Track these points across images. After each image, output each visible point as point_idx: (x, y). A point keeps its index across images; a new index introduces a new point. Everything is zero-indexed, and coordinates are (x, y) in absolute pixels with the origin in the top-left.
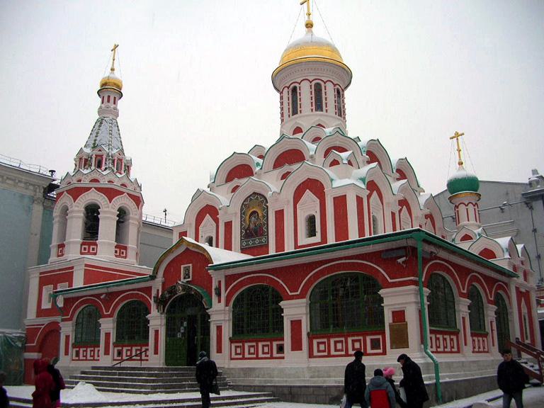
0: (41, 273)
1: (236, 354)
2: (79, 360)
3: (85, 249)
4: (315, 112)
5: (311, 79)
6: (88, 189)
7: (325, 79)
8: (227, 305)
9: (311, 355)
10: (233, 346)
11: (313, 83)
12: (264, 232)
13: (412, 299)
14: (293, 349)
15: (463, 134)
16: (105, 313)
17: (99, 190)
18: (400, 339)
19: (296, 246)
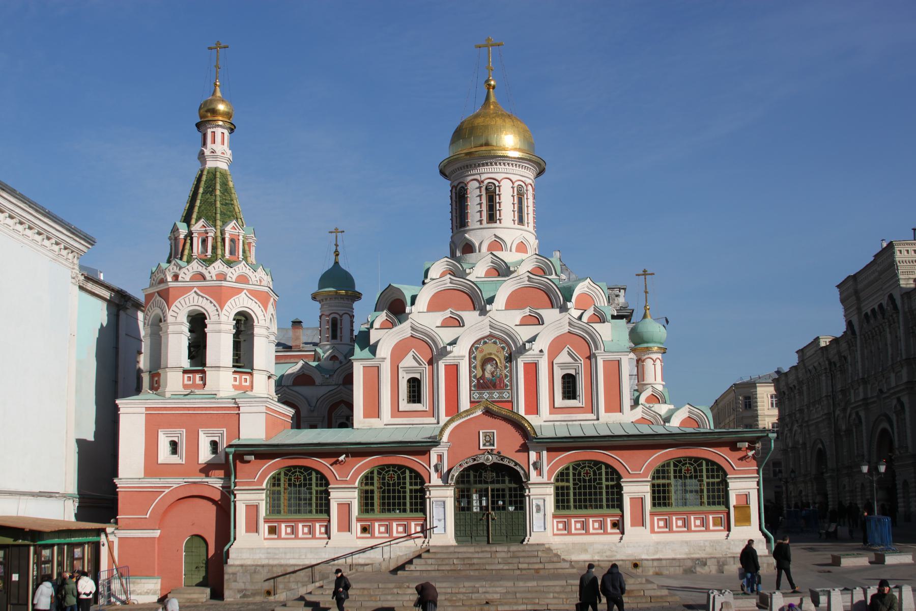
0: (146, 408)
1: (558, 529)
2: (279, 538)
3: (235, 379)
4: (517, 226)
5: (514, 178)
6: (240, 290)
8: (549, 478)
9: (653, 531)
10: (555, 521)
11: (516, 184)
12: (506, 385)
13: (754, 485)
14: (632, 525)
15: (653, 274)
16: (338, 478)
17: (252, 292)
18: (744, 519)
19: (553, 408)
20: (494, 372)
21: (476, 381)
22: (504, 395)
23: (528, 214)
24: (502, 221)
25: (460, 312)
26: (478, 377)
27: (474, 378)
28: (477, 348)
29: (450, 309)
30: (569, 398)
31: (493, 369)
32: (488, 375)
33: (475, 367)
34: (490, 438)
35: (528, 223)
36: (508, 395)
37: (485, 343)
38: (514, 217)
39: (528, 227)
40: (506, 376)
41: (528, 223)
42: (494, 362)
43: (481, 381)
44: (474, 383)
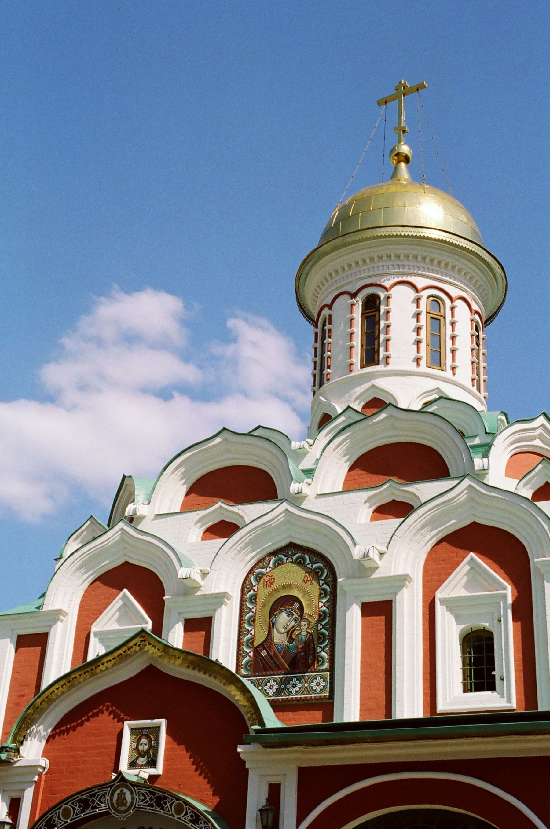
4: (423, 368)
7: (454, 292)
20: (293, 629)
21: (251, 654)
22: (313, 685)
23: (453, 351)
24: (390, 360)
25: (240, 507)
26: (256, 644)
27: (248, 646)
28: (259, 577)
29: (220, 504)
30: (479, 688)
31: (293, 623)
32: (279, 638)
33: (252, 621)
34: (150, 741)
35: (453, 369)
36: (323, 684)
37: (279, 563)
38: (418, 352)
39: (454, 374)
40: (321, 638)
41: (453, 369)
42: (296, 605)
43: (264, 653)
44: (248, 658)
